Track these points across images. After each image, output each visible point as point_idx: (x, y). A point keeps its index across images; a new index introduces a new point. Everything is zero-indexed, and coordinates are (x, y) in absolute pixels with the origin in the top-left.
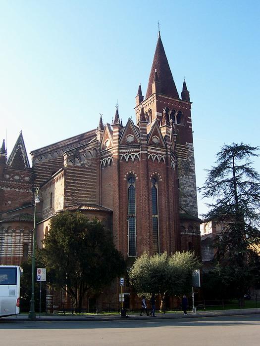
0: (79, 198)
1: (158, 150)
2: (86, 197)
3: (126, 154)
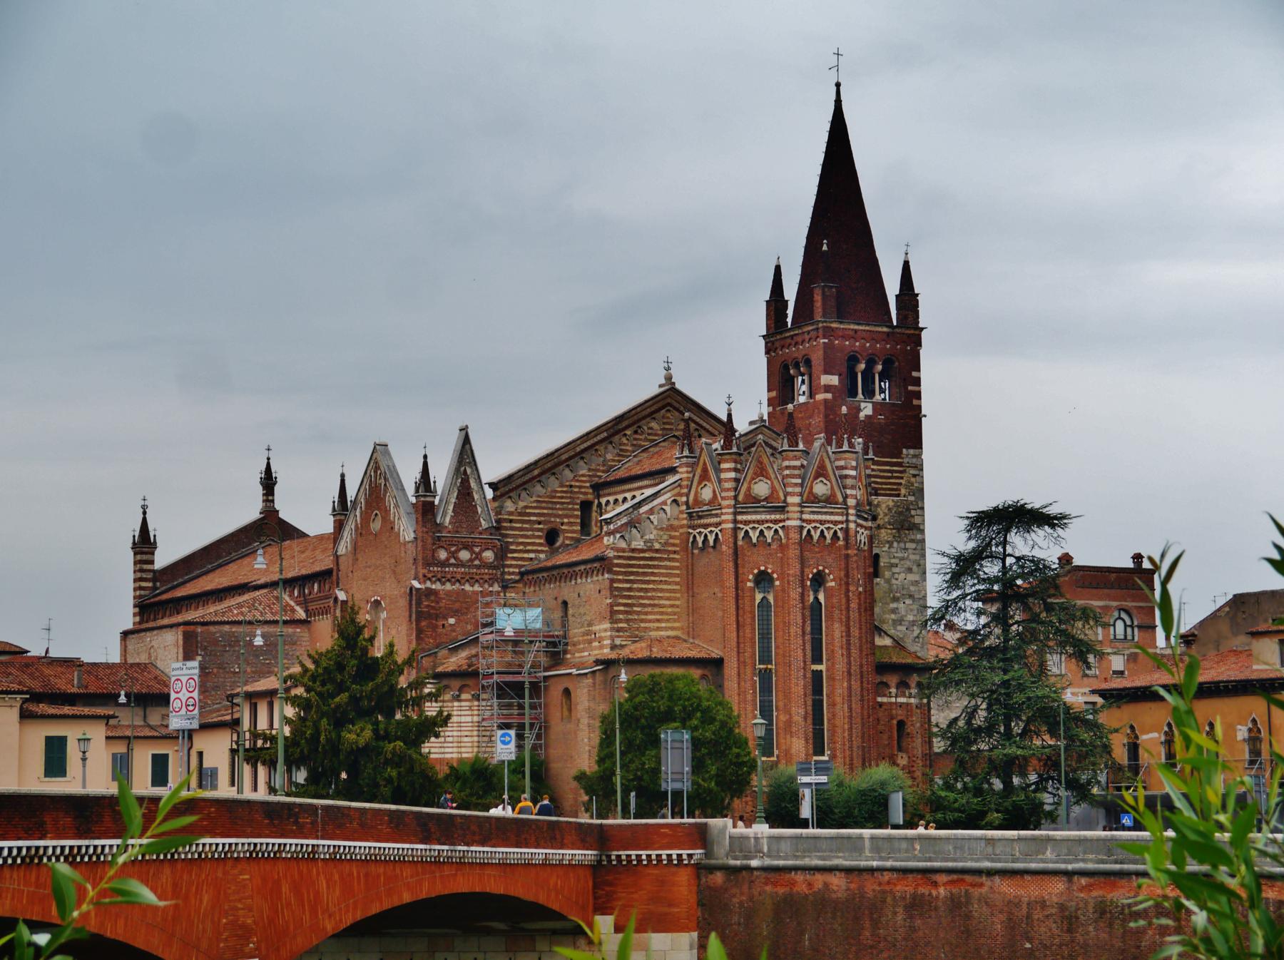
0: (642, 625)
1: (826, 513)
2: (658, 621)
3: (751, 526)
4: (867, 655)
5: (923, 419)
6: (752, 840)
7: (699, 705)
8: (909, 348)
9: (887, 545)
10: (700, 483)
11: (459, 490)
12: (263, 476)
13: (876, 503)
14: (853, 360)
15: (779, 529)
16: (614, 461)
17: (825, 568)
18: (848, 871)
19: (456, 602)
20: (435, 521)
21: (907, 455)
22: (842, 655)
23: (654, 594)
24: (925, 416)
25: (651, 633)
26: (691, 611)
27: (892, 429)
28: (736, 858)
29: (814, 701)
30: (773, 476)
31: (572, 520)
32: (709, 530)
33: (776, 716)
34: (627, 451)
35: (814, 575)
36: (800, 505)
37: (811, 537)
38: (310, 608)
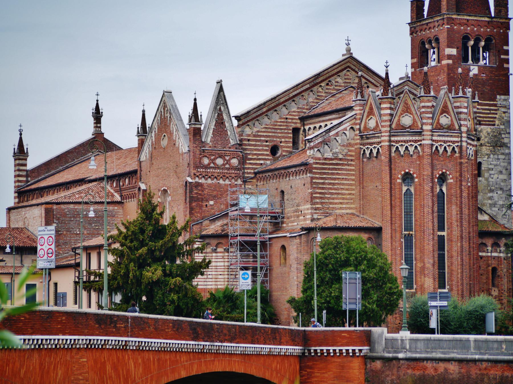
0: (331, 206)
1: (448, 136)
2: (341, 203)
3: (400, 144)
4: (473, 226)
5: (510, 76)
6: (400, 341)
7: (366, 256)
8: (502, 31)
9: (487, 157)
10: (368, 117)
11: (216, 121)
12: (94, 111)
13: (479, 129)
14: (466, 38)
15: (418, 146)
16: (313, 102)
17: (447, 171)
18: (460, 361)
19: (214, 191)
20: (201, 140)
21: (500, 99)
22: (457, 226)
23: (338, 186)
24: (512, 74)
25: (336, 211)
26: (361, 197)
27: (490, 83)
28: (389, 352)
29: (439, 254)
30: (414, 112)
31: (287, 140)
32: (373, 146)
33: (415, 264)
34: (322, 96)
35: (440, 175)
36: (431, 131)
37: (438, 151)
38: (123, 194)
